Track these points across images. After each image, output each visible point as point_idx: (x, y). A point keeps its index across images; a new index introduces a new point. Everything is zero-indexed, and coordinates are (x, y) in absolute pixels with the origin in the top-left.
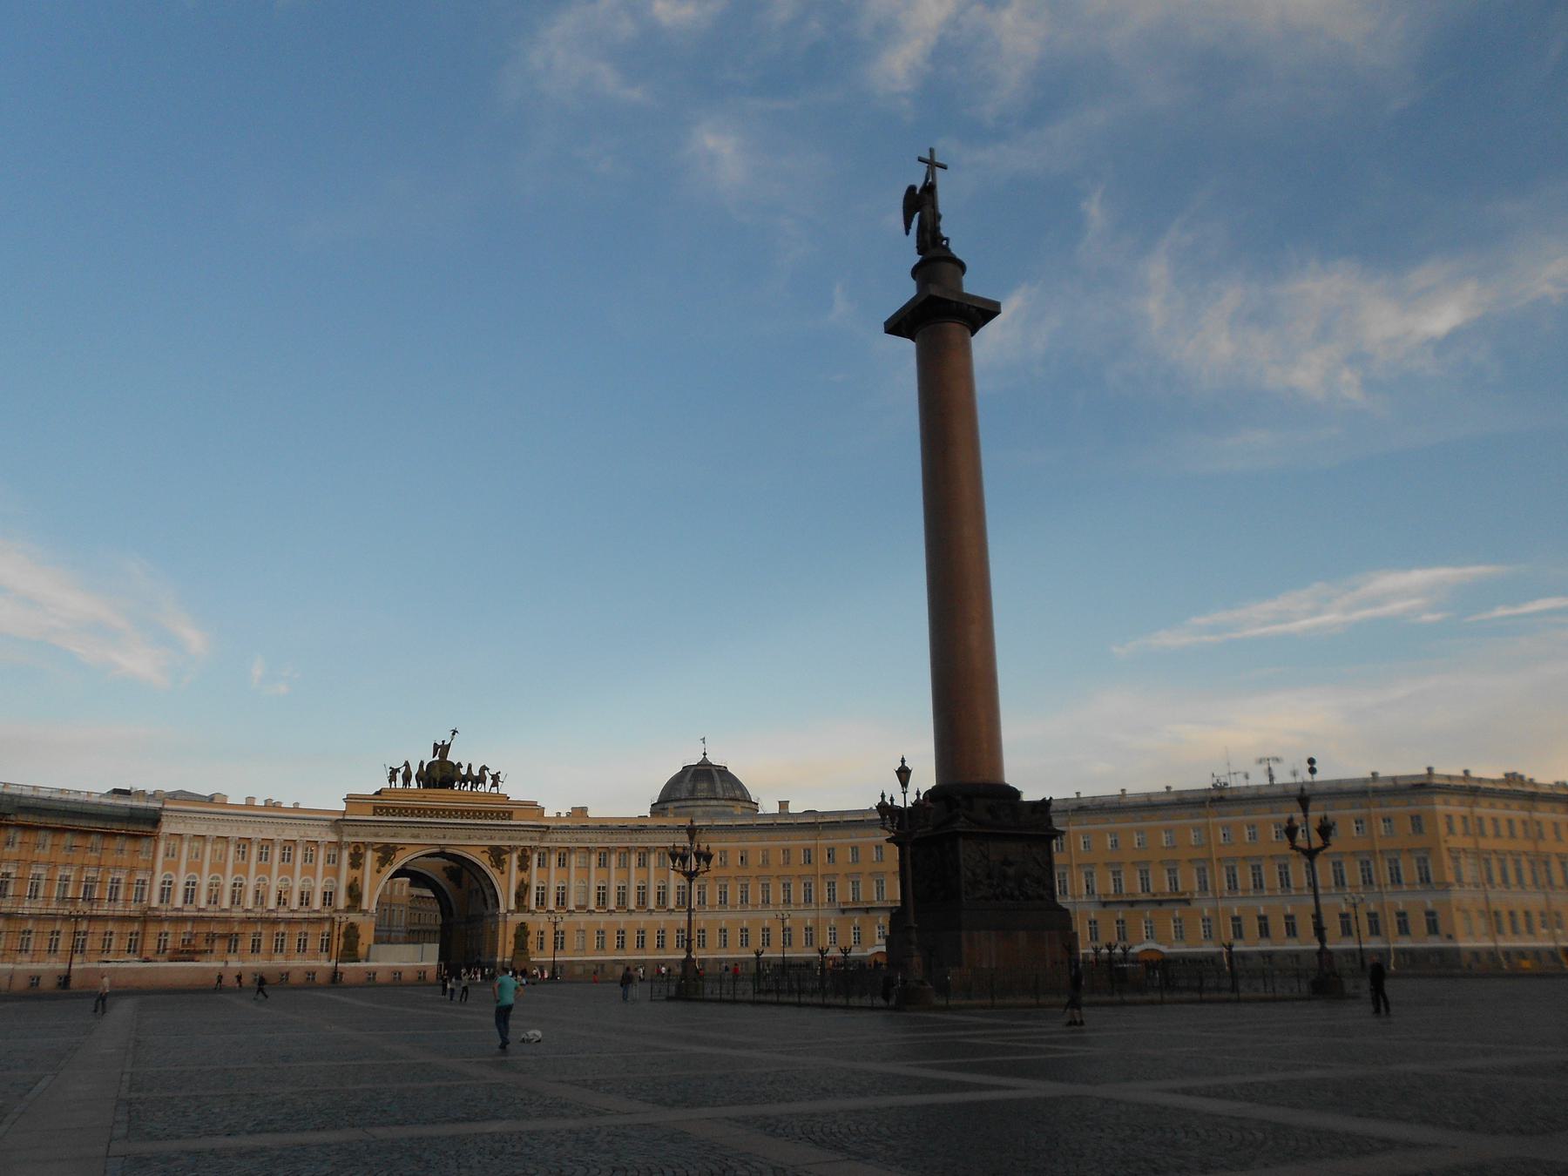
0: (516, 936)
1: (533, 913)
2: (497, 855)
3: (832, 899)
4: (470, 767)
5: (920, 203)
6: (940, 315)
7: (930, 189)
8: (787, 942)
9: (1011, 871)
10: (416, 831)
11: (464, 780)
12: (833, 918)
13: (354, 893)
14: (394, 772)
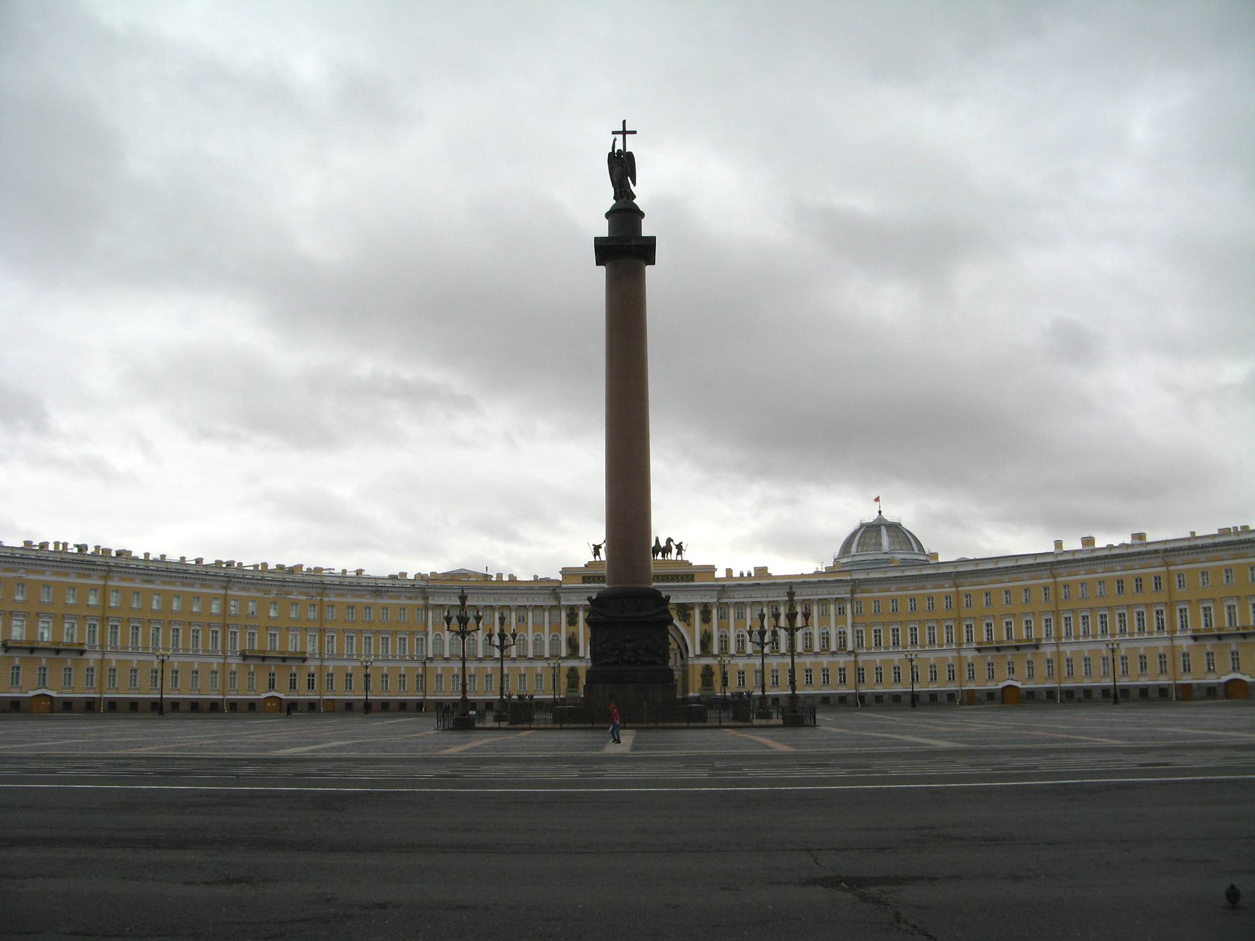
0: (703, 676)
1: (715, 656)
3: (969, 640)
8: (915, 678)
9: (629, 646)
11: (657, 549)
12: (970, 655)
13: (573, 644)
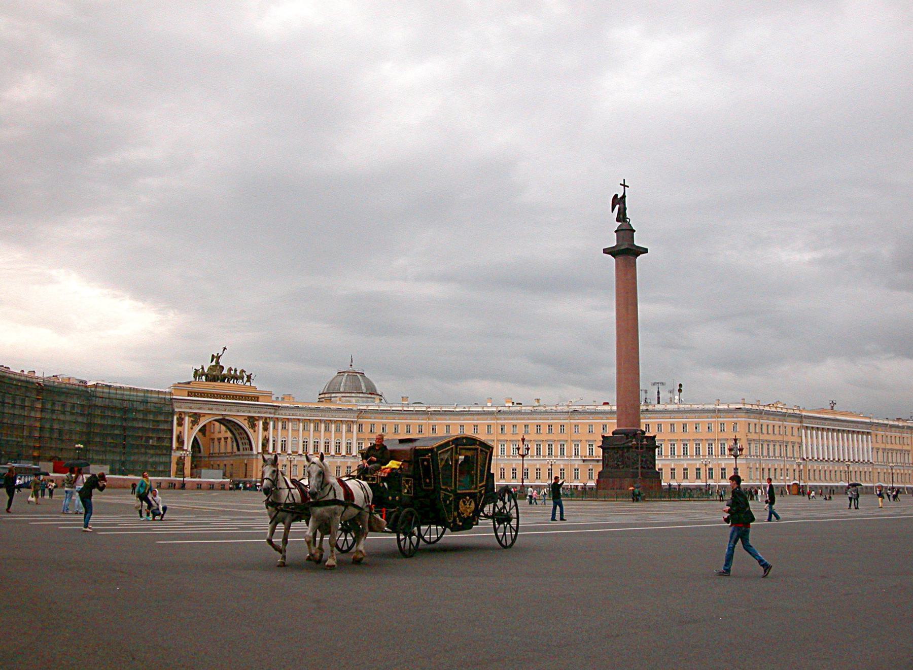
2: (252, 421)
4: (236, 371)
5: (619, 202)
6: (626, 251)
7: (624, 196)
10: (210, 406)
14: (196, 371)
